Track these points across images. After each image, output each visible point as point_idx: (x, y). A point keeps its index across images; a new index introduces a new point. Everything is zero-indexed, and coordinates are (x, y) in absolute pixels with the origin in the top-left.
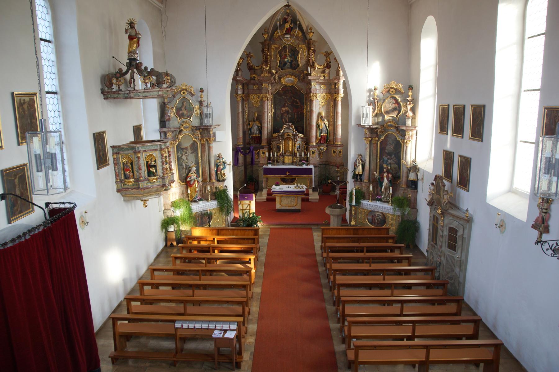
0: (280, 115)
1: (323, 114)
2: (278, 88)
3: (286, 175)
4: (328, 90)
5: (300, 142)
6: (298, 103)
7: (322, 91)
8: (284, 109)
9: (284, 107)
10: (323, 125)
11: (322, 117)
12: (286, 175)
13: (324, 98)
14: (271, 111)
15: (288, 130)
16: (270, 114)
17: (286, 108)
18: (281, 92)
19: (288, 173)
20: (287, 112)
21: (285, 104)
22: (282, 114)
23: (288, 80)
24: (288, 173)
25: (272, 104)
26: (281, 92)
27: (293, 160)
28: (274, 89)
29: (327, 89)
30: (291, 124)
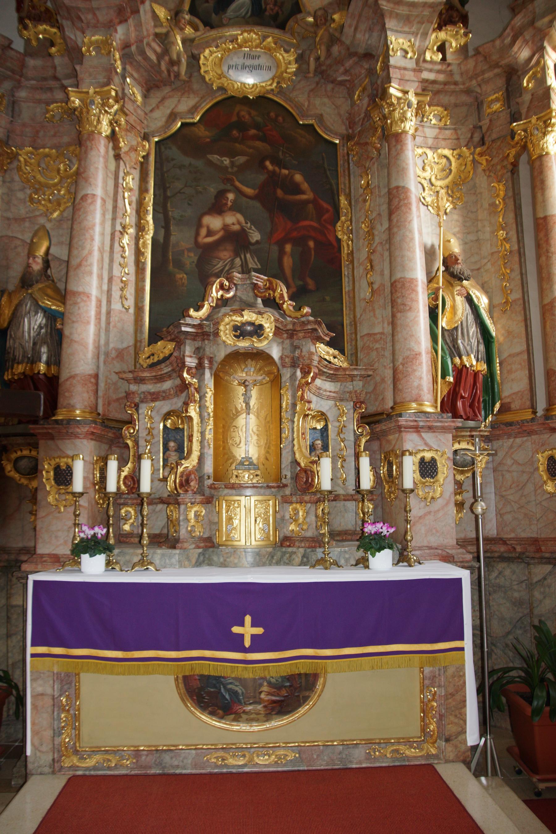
0: (190, 259)
1: (456, 248)
2: (183, 107)
3: (236, 643)
4: (465, 132)
5: (325, 406)
6: (296, 189)
7: (431, 133)
8: (214, 222)
9: (218, 208)
10: (460, 301)
11: (449, 261)
12: (236, 643)
13: (447, 171)
14: (140, 228)
15: (240, 312)
16: (126, 240)
17: (232, 220)
18: (202, 132)
19: (248, 630)
20: (237, 240)
21: (221, 194)
22: (206, 253)
23: (247, 66)
24: (248, 630)
25: (143, 190)
26: (202, 132)
27: (279, 523)
28: (159, 117)
29: (457, 122)
30: (261, 280)
